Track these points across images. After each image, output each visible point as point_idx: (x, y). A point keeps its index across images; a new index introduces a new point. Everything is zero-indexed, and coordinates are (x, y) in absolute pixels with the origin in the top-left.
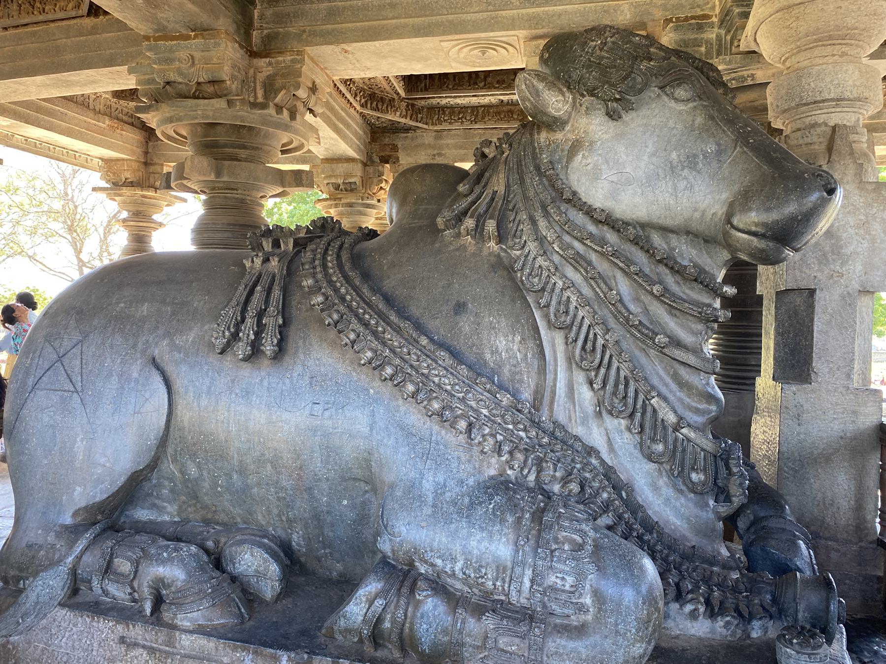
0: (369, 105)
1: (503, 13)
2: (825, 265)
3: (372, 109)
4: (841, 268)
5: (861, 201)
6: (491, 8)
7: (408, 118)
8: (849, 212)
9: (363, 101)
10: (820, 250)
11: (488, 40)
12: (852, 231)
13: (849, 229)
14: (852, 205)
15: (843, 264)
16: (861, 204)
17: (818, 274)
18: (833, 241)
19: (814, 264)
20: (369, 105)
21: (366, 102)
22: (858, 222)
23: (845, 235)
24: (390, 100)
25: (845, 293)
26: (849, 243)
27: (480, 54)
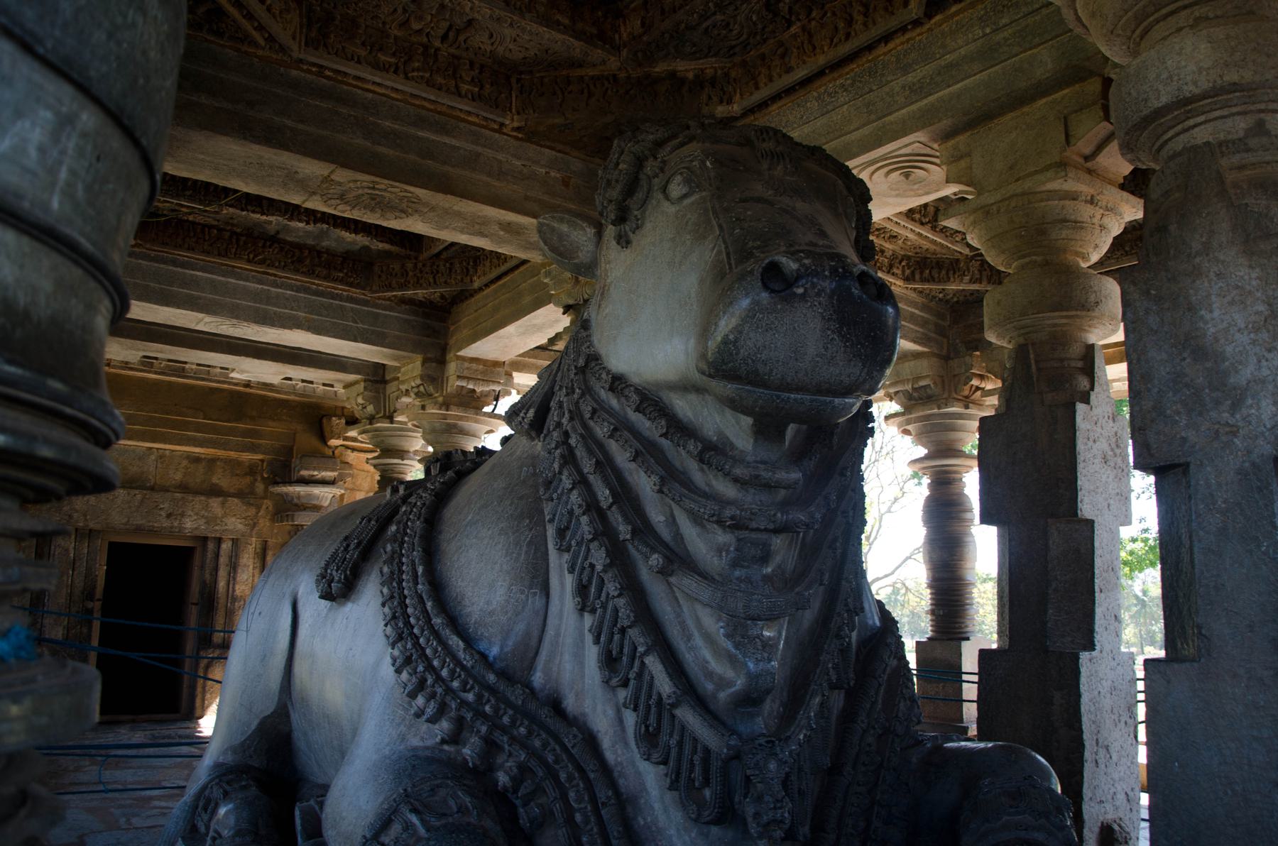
0: (917, 277)
1: (890, 118)
2: (1200, 414)
3: (923, 280)
4: (1232, 415)
5: (1254, 275)
6: (873, 117)
7: (985, 283)
8: (1232, 303)
9: (908, 272)
10: (1187, 386)
11: (886, 159)
12: (1244, 339)
13: (1238, 336)
14: (1237, 287)
15: (1236, 406)
16: (1254, 283)
17: (1191, 435)
18: (1208, 365)
19: (1178, 413)
20: (917, 277)
21: (913, 273)
22: (1253, 318)
23: (1229, 349)
24: (952, 263)
25: (1247, 464)
26: (1241, 363)
27: (902, 178)
